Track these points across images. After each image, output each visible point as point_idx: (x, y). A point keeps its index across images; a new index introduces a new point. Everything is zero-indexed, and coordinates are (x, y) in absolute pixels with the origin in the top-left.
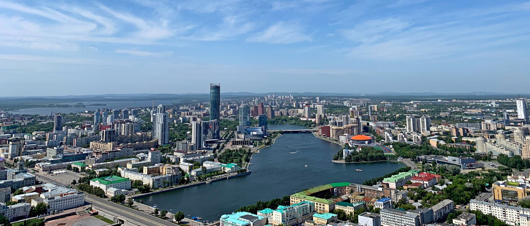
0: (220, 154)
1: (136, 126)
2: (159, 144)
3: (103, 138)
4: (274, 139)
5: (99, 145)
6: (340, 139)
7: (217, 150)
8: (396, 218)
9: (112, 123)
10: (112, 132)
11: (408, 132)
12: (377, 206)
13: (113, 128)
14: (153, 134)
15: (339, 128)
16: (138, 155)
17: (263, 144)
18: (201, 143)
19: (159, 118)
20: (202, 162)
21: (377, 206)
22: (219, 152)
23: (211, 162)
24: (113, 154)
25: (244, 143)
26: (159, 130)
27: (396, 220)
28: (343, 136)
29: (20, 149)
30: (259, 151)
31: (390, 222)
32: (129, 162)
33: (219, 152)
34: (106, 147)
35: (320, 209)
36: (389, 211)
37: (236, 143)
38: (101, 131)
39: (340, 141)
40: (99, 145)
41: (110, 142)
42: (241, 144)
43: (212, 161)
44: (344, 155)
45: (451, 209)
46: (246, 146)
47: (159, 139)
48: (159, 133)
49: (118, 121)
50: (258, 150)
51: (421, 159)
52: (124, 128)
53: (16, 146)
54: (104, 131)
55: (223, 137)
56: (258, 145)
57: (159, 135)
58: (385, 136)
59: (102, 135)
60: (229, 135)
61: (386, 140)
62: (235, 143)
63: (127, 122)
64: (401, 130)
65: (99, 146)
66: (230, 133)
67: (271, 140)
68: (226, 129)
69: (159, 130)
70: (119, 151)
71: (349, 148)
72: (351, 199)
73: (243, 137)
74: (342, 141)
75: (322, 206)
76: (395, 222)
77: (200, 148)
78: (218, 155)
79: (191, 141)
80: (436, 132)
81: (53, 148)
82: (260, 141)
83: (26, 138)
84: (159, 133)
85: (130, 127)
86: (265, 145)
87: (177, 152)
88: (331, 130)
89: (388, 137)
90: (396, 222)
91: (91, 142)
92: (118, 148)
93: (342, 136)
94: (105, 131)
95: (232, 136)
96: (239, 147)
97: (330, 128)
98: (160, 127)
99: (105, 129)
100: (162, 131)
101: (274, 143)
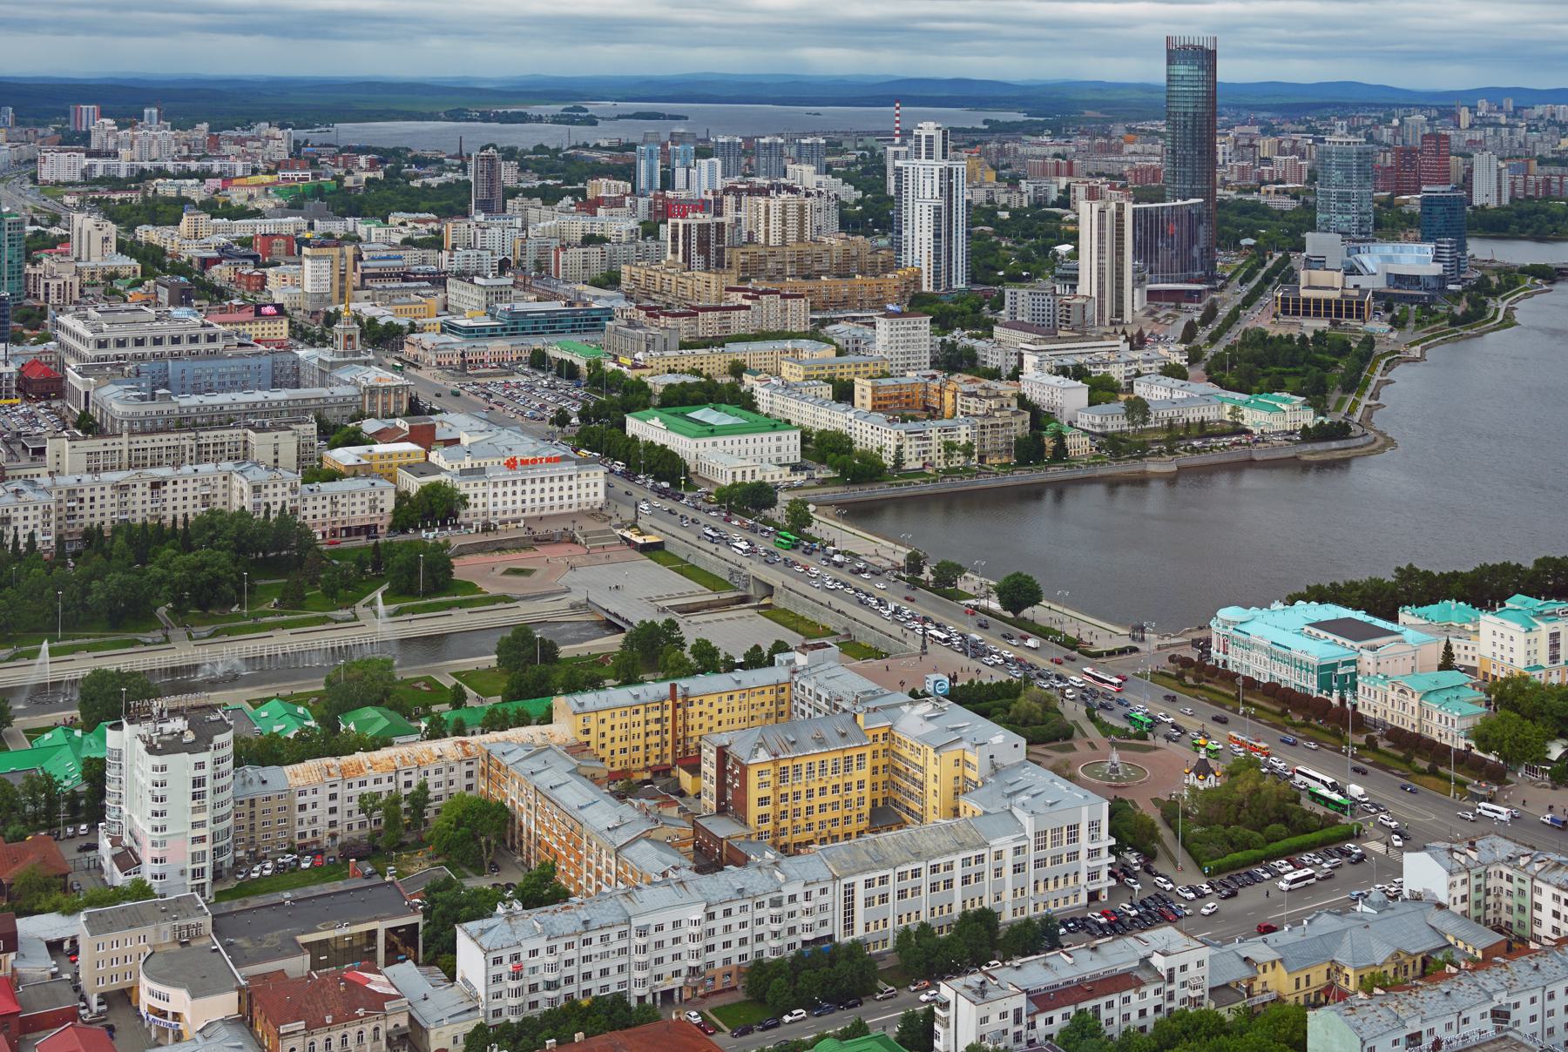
0: (1219, 348)
1: (819, 210)
2: (925, 289)
3: (675, 252)
4: (1503, 299)
5: (658, 279)
7: (1203, 334)
9: (715, 193)
10: (713, 232)
13: (719, 213)
14: (896, 246)
16: (830, 328)
17: (1443, 319)
18: (1122, 297)
20: (1126, 378)
22: (1213, 339)
23: (1170, 379)
24: (720, 319)
26: (925, 228)
29: (343, 277)
30: (1418, 348)
32: (790, 355)
33: (1213, 339)
34: (690, 290)
38: (666, 223)
40: (658, 279)
41: (707, 269)
42: (1328, 315)
43: (1179, 377)
46: (1354, 322)
47: (925, 268)
48: (925, 242)
49: (739, 186)
50: (1412, 345)
52: (767, 212)
53: (326, 264)
54: (681, 222)
55: (1231, 277)
56: (1411, 325)
57: (925, 251)
59: (669, 239)
60: (1263, 271)
62: (1294, 307)
63: (779, 192)
65: (658, 283)
66: (1270, 264)
67: (1485, 303)
68: (1251, 242)
69: (925, 228)
70: (748, 308)
73: (1338, 284)
78: (1209, 353)
79: (1073, 287)
81: (472, 282)
82: (1425, 307)
83: (364, 238)
84: (925, 242)
85: (792, 212)
86: (1451, 324)
87: (1006, 325)
91: (623, 267)
92: (740, 294)
94: (685, 226)
98: (925, 217)
99: (683, 216)
100: (937, 235)
101: (1500, 317)
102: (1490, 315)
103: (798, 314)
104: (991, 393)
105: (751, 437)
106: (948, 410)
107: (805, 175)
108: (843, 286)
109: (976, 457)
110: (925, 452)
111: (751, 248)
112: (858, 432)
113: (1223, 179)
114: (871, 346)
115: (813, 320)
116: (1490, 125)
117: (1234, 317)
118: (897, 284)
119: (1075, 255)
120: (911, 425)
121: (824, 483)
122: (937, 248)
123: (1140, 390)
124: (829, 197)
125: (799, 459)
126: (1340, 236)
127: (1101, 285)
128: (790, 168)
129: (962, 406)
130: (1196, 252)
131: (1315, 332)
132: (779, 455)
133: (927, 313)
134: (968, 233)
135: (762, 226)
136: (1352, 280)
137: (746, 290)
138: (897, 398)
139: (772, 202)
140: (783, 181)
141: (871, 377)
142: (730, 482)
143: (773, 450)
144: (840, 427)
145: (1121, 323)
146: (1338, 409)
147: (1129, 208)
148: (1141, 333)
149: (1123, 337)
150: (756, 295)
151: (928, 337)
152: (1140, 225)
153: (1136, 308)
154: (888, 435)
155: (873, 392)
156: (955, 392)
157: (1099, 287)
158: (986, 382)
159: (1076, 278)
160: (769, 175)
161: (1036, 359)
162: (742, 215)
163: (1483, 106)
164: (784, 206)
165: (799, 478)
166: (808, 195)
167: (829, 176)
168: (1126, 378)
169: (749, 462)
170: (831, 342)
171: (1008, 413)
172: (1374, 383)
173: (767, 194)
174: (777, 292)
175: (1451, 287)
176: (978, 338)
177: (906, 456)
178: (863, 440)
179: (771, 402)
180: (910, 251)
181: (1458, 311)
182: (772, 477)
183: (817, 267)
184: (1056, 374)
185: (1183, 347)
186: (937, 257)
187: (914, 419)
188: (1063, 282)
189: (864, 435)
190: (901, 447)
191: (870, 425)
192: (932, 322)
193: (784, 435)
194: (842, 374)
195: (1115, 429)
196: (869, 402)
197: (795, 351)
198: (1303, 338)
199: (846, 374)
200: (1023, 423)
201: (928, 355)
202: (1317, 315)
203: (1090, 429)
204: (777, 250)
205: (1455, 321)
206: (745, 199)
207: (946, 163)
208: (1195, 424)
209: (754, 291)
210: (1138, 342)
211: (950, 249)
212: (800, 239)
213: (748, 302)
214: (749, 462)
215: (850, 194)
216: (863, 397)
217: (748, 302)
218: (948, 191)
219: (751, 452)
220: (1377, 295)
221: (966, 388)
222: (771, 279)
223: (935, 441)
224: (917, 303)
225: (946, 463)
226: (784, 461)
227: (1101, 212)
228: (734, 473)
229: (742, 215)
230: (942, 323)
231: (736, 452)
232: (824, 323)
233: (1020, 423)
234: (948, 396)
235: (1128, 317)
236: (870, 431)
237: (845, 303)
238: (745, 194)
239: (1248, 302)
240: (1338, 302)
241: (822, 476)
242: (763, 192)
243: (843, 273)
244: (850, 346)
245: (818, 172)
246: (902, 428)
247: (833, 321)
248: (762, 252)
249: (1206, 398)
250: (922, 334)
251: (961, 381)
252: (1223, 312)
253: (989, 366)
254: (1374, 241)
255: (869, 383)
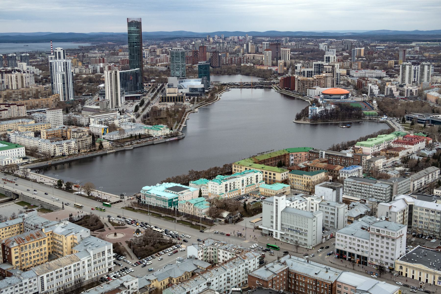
0: (145, 113)
1: (28, 77)
4: (219, 94)
6: (308, 93)
7: (141, 109)
8: (363, 188)
11: (400, 83)
12: (342, 174)
15: (307, 79)
16: (33, 115)
17: (204, 101)
18: (118, 99)
19: (58, 66)
20: (119, 123)
21: (342, 174)
25: (177, 99)
27: (363, 191)
28: (312, 90)
31: (355, 193)
33: (143, 110)
35: (270, 179)
36: (354, 181)
37: (166, 99)
39: (308, 96)
42: (174, 101)
44: (309, 114)
45: (435, 177)
46: (181, 103)
49: (2, 71)
51: (411, 118)
55: (149, 91)
56: (195, 102)
58: (368, 90)
61: (369, 94)
62: (164, 99)
63: (15, 72)
64: (390, 81)
66: (159, 87)
70: (7, 110)
71: (319, 106)
72: (311, 168)
74: (310, 96)
75: (272, 176)
76: (361, 192)
77: (117, 105)
79: (104, 97)
80: (438, 83)
88: (296, 82)
89: (371, 90)
90: (363, 193)
92: (4, 106)
93: (311, 90)
95: (162, 90)
96: (170, 104)
97: (296, 79)
100: (64, 84)
102: (216, 98)
103: (23, 111)
104: (81, 131)
105: (10, 150)
106: (69, 137)
107: (24, 66)
108: (37, 101)
109: (77, 150)
110: (62, 150)
111: (7, 91)
112: (42, 146)
113: (146, 62)
114: (45, 119)
115: (28, 112)
116: (218, 43)
117: (149, 103)
118: (53, 99)
119: (104, 87)
120: (58, 143)
121: (33, 162)
122: (64, 87)
123: (123, 127)
124: (31, 73)
125: (25, 156)
126: (177, 78)
127: (112, 96)
128: (19, 63)
129: (72, 135)
130: (138, 85)
131: (170, 106)
132: (19, 155)
133: (61, 108)
134: (73, 82)
135: (10, 83)
136: (180, 91)
137: (6, 104)
138: (54, 134)
139: (12, 75)
140: (16, 68)
141: (46, 129)
142: (4, 165)
143: (17, 153)
144: (37, 145)
145: (118, 107)
146: (176, 128)
147: (118, 72)
148: (123, 110)
149: (118, 111)
150: (9, 105)
151: (62, 115)
152: (122, 77)
153: (122, 102)
154: (51, 146)
155: (46, 133)
156: (70, 131)
157: (111, 97)
158: (79, 128)
159: (105, 94)
160: (12, 66)
161: (93, 120)
162: (4, 80)
163: (216, 37)
164: (16, 76)
165: (26, 161)
166: (24, 72)
167: (31, 66)
168: (119, 123)
169: (9, 158)
170: (33, 119)
171: (85, 137)
172: (185, 120)
173: (11, 73)
174: (16, 104)
175: (206, 91)
176: (77, 115)
177: (57, 152)
178: (44, 149)
179: (16, 139)
180: (56, 89)
181: (208, 97)
182: (17, 162)
183: (28, 95)
184: (99, 124)
185: (134, 113)
186: (64, 90)
187: (59, 141)
188: (101, 96)
189: (44, 147)
190: (55, 149)
191: (45, 144)
192: (63, 110)
193: (20, 149)
194: (37, 128)
195: (116, 139)
196: (45, 136)
197: (22, 122)
198: (167, 109)
199: (38, 128)
200: (90, 139)
201: (62, 121)
202: (171, 101)
203: (109, 139)
204: (15, 91)
205: (208, 101)
206: (5, 75)
207: (65, 61)
208: (138, 135)
209: (8, 104)
210: (122, 112)
211: (68, 87)
212: (23, 87)
213: (7, 108)
214: (9, 158)
215: (38, 71)
216: (44, 135)
217: (7, 108)
218: (66, 69)
219: (10, 155)
220: (187, 95)
221: (73, 130)
222: (14, 100)
223: (65, 146)
224: (59, 105)
225: (69, 153)
226: (20, 156)
227: (111, 74)
228: (5, 162)
229: (4, 80)
230: (66, 111)
231: (5, 155)
232: (30, 113)
233: (89, 139)
234: (68, 133)
235: (120, 105)
236: (46, 145)
237: (37, 106)
238: (4, 73)
239: (153, 99)
240: (176, 97)
241: (32, 160)
242: (10, 72)
243: (36, 96)
244: (39, 120)
245: (28, 65)
246: (54, 144)
247: (33, 112)
248: (11, 92)
249: (141, 128)
250: (60, 115)
251: (73, 128)
252: (146, 102)
253: (80, 123)
254: (186, 79)
255: (45, 131)
